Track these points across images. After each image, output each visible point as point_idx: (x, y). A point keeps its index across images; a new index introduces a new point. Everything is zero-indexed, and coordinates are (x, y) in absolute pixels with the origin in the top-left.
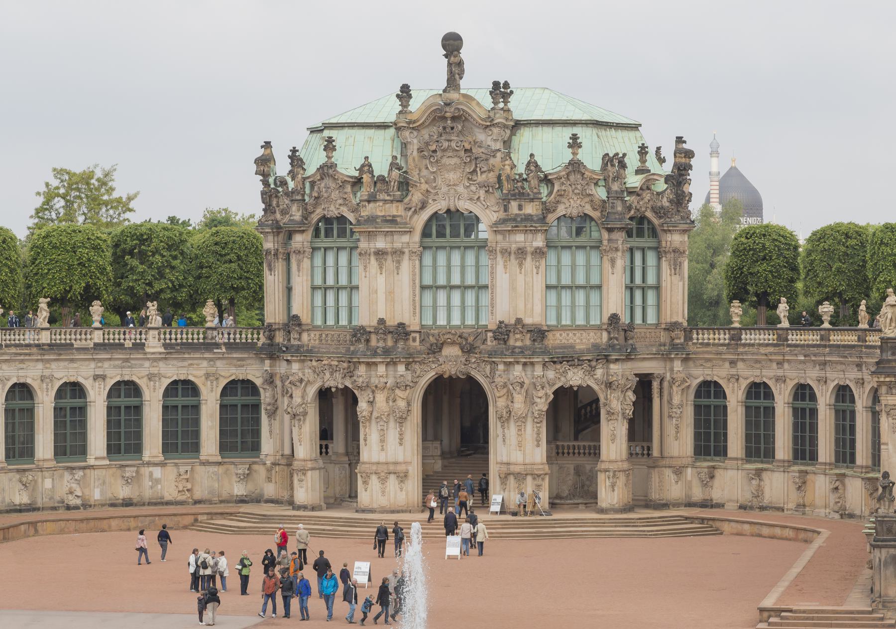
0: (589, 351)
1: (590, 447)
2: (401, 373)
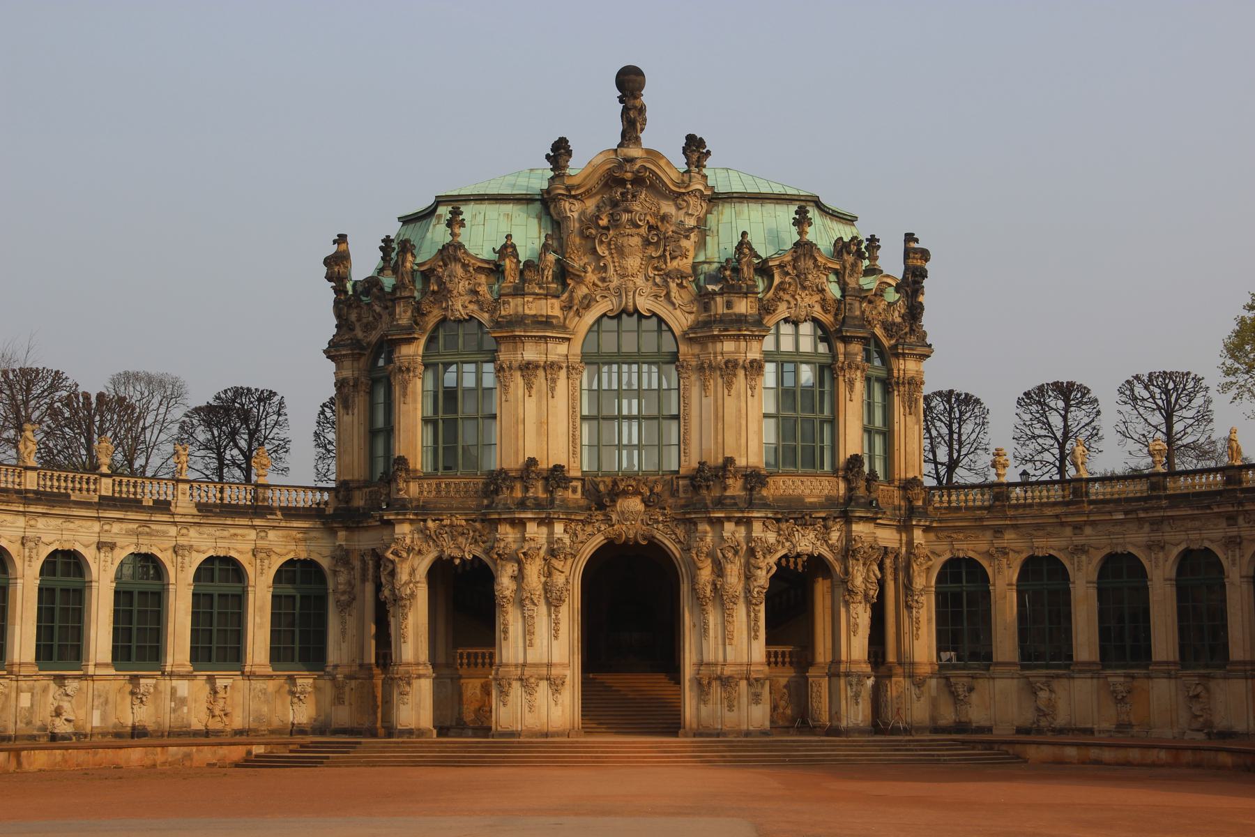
0: (822, 506)
1: (783, 654)
2: (559, 536)
